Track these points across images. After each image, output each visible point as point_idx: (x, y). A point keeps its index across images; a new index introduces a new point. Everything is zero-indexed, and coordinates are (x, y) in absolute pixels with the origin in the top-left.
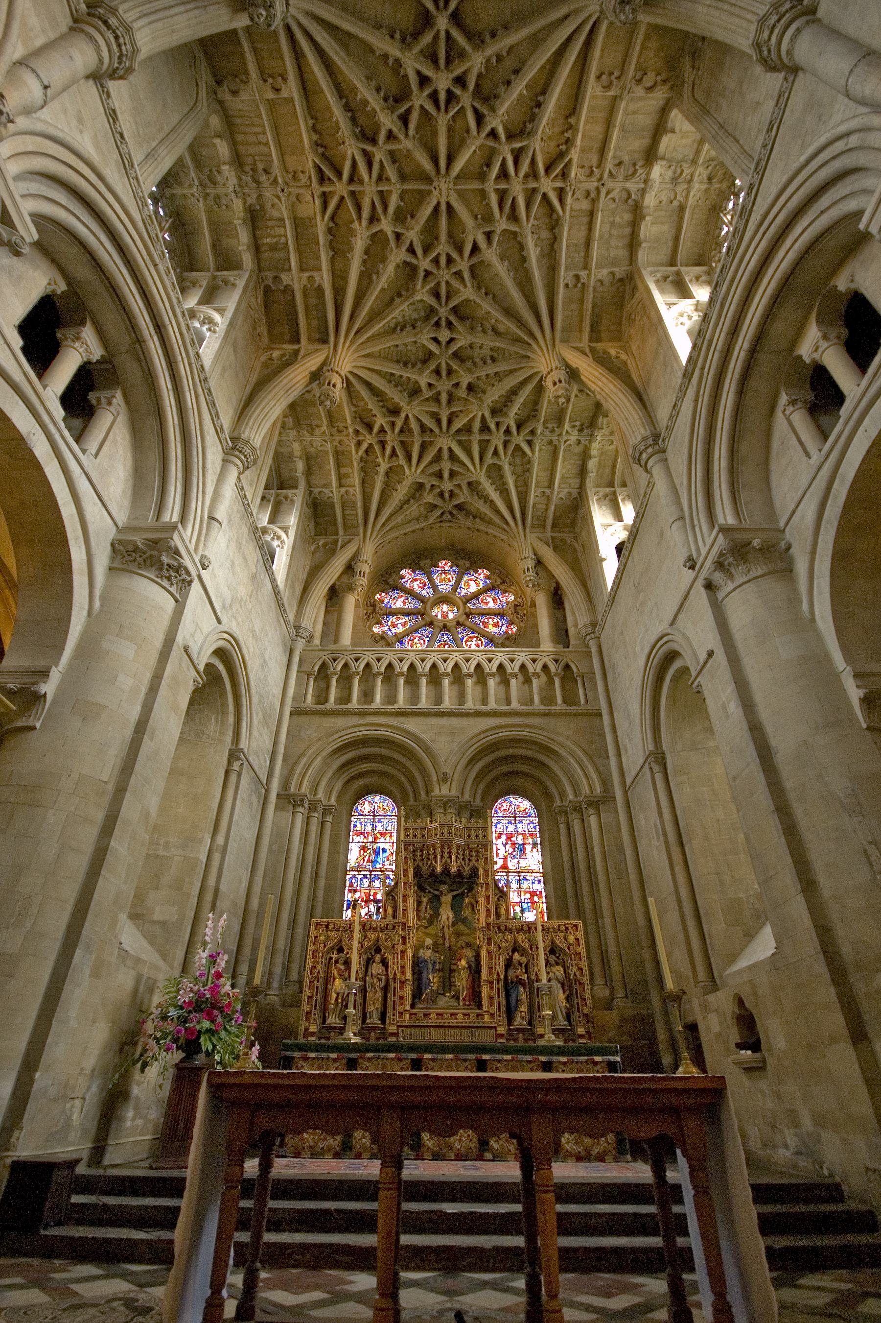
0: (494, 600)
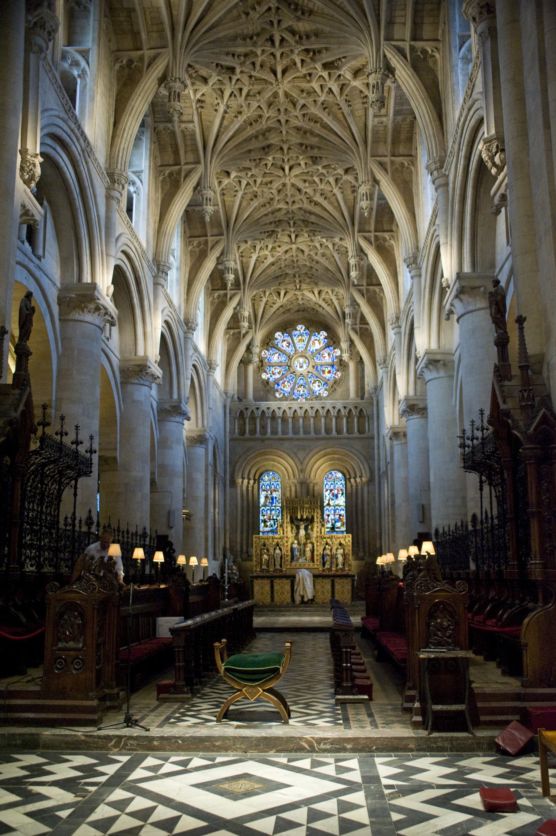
0: (329, 355)
